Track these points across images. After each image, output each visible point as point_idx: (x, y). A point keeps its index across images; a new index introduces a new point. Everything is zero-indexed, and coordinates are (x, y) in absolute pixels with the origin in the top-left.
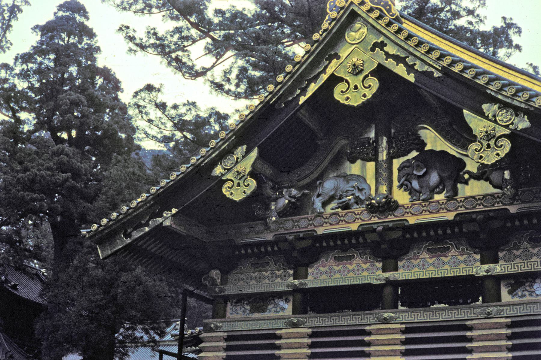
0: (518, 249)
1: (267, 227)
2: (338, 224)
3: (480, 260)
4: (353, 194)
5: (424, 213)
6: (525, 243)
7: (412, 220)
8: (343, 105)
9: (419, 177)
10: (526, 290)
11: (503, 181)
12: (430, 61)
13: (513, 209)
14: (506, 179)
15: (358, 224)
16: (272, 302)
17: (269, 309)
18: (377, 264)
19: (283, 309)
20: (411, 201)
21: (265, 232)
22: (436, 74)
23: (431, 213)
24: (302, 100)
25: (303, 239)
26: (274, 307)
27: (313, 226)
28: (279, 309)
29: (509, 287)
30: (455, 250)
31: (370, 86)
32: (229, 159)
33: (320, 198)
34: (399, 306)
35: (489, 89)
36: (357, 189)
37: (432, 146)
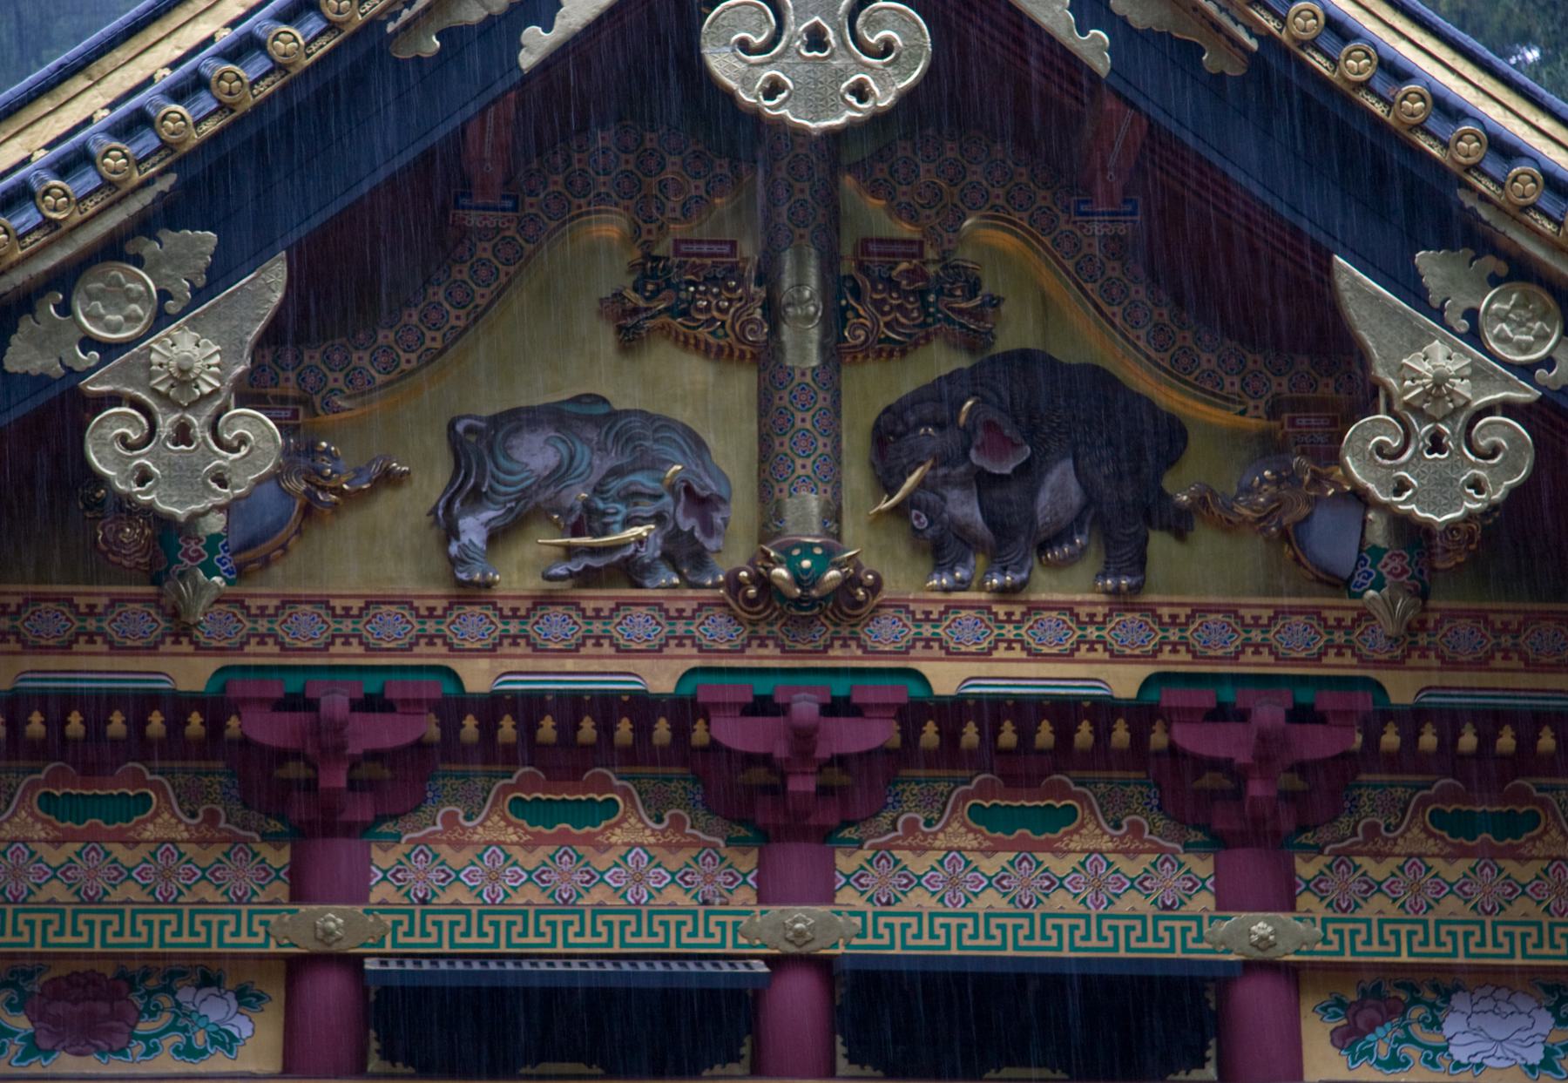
0: (1379, 856)
1: (181, 630)
2: (573, 651)
3: (1215, 884)
4: (659, 518)
5: (1000, 653)
6: (1416, 831)
7: (946, 678)
8: (756, 115)
10: (1410, 1039)
11: (1360, 558)
13: (1402, 689)
14: (1377, 552)
15: (682, 666)
16: (165, 1001)
17: (146, 1038)
18: (732, 855)
19: (226, 1042)
20: (946, 590)
21: (168, 646)
23: (1034, 656)
26: (172, 1027)
28: (200, 1040)
29: (1336, 1015)
31: (887, 47)
34: (842, 1065)
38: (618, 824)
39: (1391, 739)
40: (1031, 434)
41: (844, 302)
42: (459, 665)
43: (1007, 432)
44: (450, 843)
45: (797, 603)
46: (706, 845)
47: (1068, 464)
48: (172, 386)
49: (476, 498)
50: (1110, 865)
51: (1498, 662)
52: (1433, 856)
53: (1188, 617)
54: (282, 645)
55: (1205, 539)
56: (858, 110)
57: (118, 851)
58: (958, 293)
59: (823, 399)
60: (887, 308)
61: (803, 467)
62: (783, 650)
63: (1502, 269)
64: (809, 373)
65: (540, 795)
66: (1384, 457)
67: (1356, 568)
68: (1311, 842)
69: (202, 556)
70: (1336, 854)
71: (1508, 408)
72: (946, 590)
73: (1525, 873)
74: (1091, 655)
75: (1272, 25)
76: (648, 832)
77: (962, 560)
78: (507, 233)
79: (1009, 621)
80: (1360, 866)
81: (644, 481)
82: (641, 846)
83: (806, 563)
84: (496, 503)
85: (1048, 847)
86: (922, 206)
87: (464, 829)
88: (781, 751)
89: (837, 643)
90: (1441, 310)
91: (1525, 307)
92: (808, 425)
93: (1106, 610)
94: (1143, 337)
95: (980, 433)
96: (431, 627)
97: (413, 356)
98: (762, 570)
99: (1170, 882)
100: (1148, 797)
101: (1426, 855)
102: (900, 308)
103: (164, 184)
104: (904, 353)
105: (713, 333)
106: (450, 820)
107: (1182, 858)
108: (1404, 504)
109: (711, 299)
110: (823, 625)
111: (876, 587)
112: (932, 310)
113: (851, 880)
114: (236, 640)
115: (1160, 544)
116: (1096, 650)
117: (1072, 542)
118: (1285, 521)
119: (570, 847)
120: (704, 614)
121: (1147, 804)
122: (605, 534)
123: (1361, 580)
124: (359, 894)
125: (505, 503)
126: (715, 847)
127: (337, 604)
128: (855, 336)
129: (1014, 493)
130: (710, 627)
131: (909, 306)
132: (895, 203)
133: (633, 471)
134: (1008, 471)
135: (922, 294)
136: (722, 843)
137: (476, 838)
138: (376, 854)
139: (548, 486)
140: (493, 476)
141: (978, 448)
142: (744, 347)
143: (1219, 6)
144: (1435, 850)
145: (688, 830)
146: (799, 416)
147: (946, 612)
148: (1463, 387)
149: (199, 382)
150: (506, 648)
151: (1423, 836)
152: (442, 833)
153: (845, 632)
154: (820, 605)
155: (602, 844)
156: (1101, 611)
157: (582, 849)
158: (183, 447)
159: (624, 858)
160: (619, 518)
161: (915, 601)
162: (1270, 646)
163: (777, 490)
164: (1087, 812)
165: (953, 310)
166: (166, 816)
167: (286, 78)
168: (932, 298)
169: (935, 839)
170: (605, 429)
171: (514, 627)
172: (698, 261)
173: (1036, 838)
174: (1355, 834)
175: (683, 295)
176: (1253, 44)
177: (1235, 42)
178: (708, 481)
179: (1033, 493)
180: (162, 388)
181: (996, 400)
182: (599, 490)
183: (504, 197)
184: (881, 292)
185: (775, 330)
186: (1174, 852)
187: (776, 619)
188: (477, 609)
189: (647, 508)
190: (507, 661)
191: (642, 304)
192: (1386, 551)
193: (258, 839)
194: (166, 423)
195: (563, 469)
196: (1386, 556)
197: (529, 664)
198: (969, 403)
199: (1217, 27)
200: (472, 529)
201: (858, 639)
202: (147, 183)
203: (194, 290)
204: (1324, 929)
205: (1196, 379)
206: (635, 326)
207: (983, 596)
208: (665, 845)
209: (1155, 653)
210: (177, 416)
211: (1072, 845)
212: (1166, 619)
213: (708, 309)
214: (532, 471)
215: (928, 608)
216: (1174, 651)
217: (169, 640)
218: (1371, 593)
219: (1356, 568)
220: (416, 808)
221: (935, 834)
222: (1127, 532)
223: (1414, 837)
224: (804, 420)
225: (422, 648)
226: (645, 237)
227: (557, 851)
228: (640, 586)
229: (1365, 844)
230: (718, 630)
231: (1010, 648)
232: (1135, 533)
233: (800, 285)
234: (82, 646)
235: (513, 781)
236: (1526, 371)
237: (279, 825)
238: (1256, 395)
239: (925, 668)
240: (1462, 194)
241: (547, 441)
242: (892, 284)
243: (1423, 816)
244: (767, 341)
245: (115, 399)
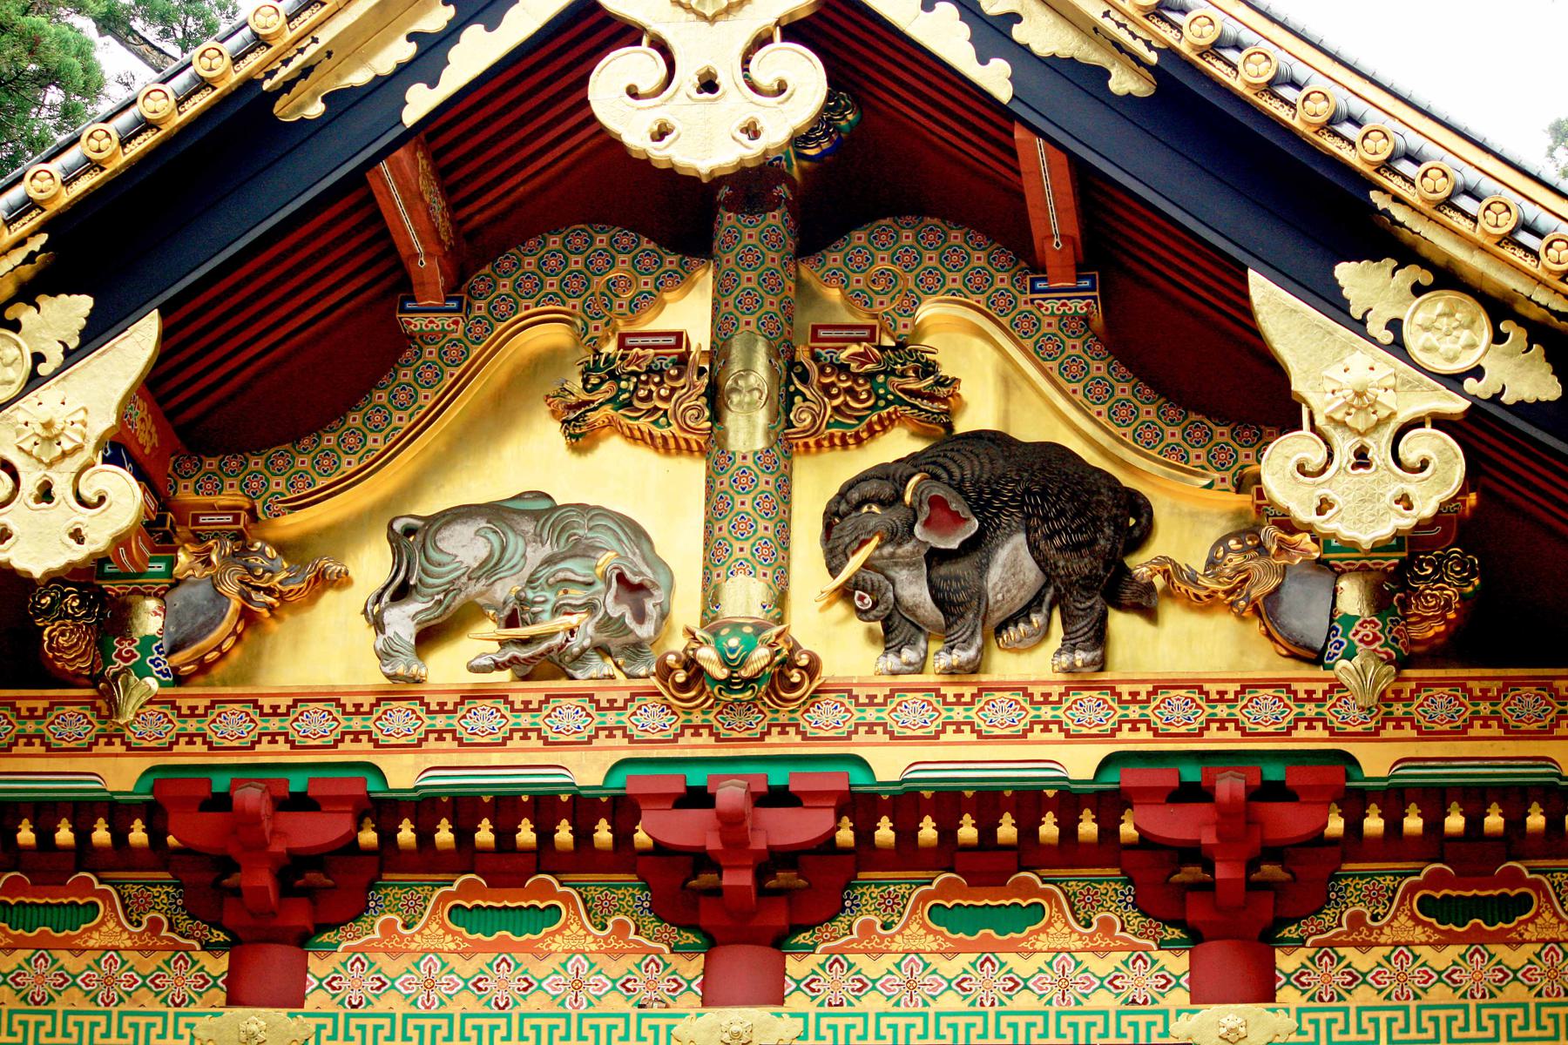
0: (1365, 946)
3: (1190, 981)
4: (590, 607)
6: (1403, 918)
9: (935, 557)
11: (1332, 628)
12: (1106, 14)
14: (1349, 620)
18: (677, 962)
20: (894, 673)
22: (1123, 82)
24: (419, 102)
25: (301, 803)
27: (365, 744)
31: (781, 89)
33: (413, 607)
35: (1385, 191)
36: (614, 583)
37: (1006, 416)
38: (559, 931)
39: (1374, 824)
40: (979, 508)
41: (792, 389)
42: (383, 761)
43: (953, 507)
44: (386, 951)
45: (727, 684)
46: (647, 951)
47: (1020, 539)
48: (36, 444)
49: (402, 593)
50: (1078, 964)
51: (1476, 730)
52: (1421, 944)
53: (1149, 694)
54: (211, 746)
55: (1174, 617)
56: (747, 147)
57: (65, 958)
58: (911, 373)
59: (766, 483)
60: (835, 391)
61: (741, 549)
62: (718, 739)
63: (1427, 278)
64: (750, 458)
65: (480, 902)
66: (1305, 474)
67: (1328, 639)
68: (1295, 936)
69: (135, 656)
70: (1318, 945)
71: (1441, 422)
72: (894, 673)
73: (1515, 958)
74: (1046, 736)
75: (1170, 36)
76: (590, 939)
77: (910, 642)
79: (958, 703)
80: (1344, 957)
81: (576, 568)
82: (583, 952)
83: (733, 642)
84: (424, 596)
85: (1011, 947)
86: (877, 293)
87: (402, 937)
88: (713, 843)
89: (775, 730)
90: (1363, 322)
91: (1450, 315)
92: (748, 508)
94: (1105, 413)
95: (926, 508)
96: (357, 723)
97: (354, 459)
98: (691, 653)
99: (1142, 981)
100: (1122, 893)
101: (1413, 944)
102: (850, 391)
103: (36, 244)
104: (859, 441)
105: (655, 422)
106: (388, 927)
107: (1156, 954)
108: (1325, 524)
109: (653, 388)
110: (760, 712)
111: (812, 669)
112: (881, 391)
113: (802, 986)
114: (165, 741)
115: (1121, 624)
116: (1050, 731)
117: (1029, 622)
118: (1254, 593)
119: (508, 953)
120: (636, 704)
121: (1120, 901)
122: (533, 623)
123: (1333, 650)
124: (295, 1000)
125: (432, 596)
126: (659, 952)
127: (266, 703)
128: (802, 418)
129: (961, 569)
130: (640, 719)
131: (859, 389)
132: (849, 289)
133: (564, 559)
134: (954, 545)
136: (667, 950)
137: (413, 946)
138: (313, 962)
139: (478, 579)
140: (424, 570)
141: (927, 524)
142: (688, 436)
143: (1117, 23)
144: (1424, 938)
145: (632, 936)
146: (738, 499)
147: (891, 695)
148: (1388, 400)
149: (62, 439)
150: (432, 742)
151: (1410, 923)
152: (380, 941)
153: (783, 718)
154: (753, 688)
155: (541, 951)
156: (1056, 690)
157: (519, 957)
159: (564, 965)
160: (548, 607)
161: (859, 685)
162: (1236, 721)
163: (715, 574)
164: (1055, 909)
165: (903, 391)
167: (159, 134)
168: (881, 378)
169: (893, 941)
170: (541, 522)
171: (440, 722)
172: (641, 352)
173: (1000, 938)
174: (1340, 925)
175: (623, 384)
176: (1153, 58)
177: (1136, 59)
178: (645, 569)
179: (983, 569)
180: (26, 446)
181: (945, 476)
182: (531, 581)
183: (448, 299)
184: (827, 376)
185: (717, 417)
186: (1147, 949)
187: (711, 707)
189: (577, 595)
190: (432, 756)
191: (585, 397)
192: (1357, 618)
193: (198, 947)
194: (30, 483)
195: (495, 560)
196: (1357, 623)
197: (455, 759)
198: (916, 479)
199: (1119, 46)
200: (403, 621)
201: (797, 726)
202: (21, 242)
203: (67, 353)
204: (1299, 1019)
205: (1160, 453)
206: (576, 419)
208: (606, 952)
209: (1113, 732)
210: (42, 473)
211: (1038, 946)
212: (1126, 697)
213: (649, 398)
214: (462, 562)
215: (872, 691)
216: (1134, 729)
218: (1344, 663)
219: (1328, 639)
220: (356, 918)
221: (892, 936)
222: (1083, 606)
223: (1403, 926)
224: (745, 503)
225: (347, 745)
226: (592, 333)
227: (495, 959)
228: (572, 678)
229: (1348, 934)
230: (652, 719)
231: (958, 731)
232: (1091, 607)
233: (748, 370)
234: (21, 748)
235: (454, 888)
236: (1454, 381)
237: (222, 935)
238: (1222, 467)
240: (1375, 196)
241: (477, 533)
242: (843, 368)
243: (1411, 904)
244: (711, 429)
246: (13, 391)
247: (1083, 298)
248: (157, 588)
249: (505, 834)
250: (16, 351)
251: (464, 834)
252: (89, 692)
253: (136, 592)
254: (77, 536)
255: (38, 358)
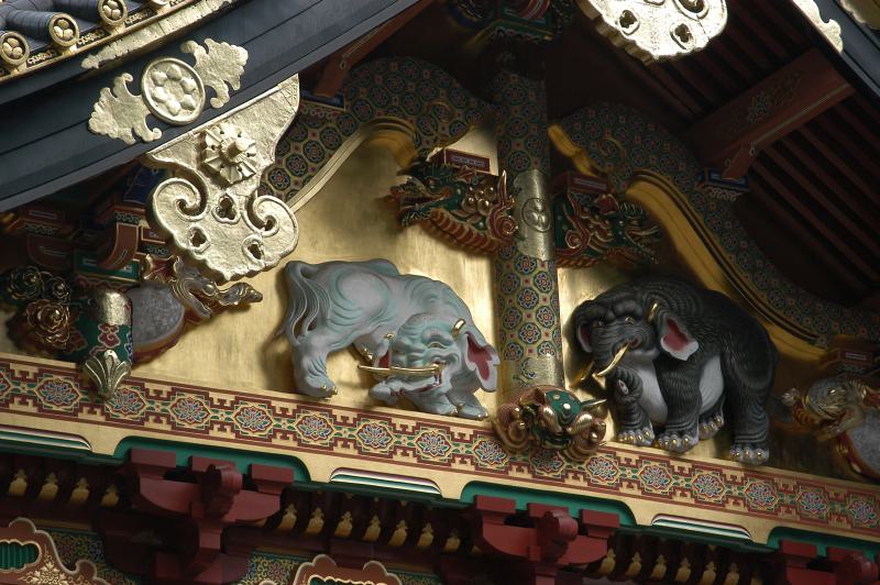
23: (699, 503)
30: (56, 565)
32: (173, 78)
40: (695, 335)
42: (307, 458)
56: (684, 48)
69: (117, 342)
78: (330, 125)
93: (742, 474)
105: (476, 225)
110: (559, 459)
112: (620, 233)
122: (409, 367)
135: (613, 220)
153: (576, 468)
158: (226, 219)
166: (50, 565)
179: (698, 377)
182: (405, 330)
188: (317, 414)
207: (660, 452)
217: (85, 409)
230: (489, 454)
239: (628, 501)
245: (175, 170)
246: (194, 115)
247: (737, 191)
248: (123, 285)
249: (360, 526)
250: (195, 84)
251: (331, 521)
252: (72, 365)
253: (105, 284)
254: (256, 251)
255: (211, 93)
